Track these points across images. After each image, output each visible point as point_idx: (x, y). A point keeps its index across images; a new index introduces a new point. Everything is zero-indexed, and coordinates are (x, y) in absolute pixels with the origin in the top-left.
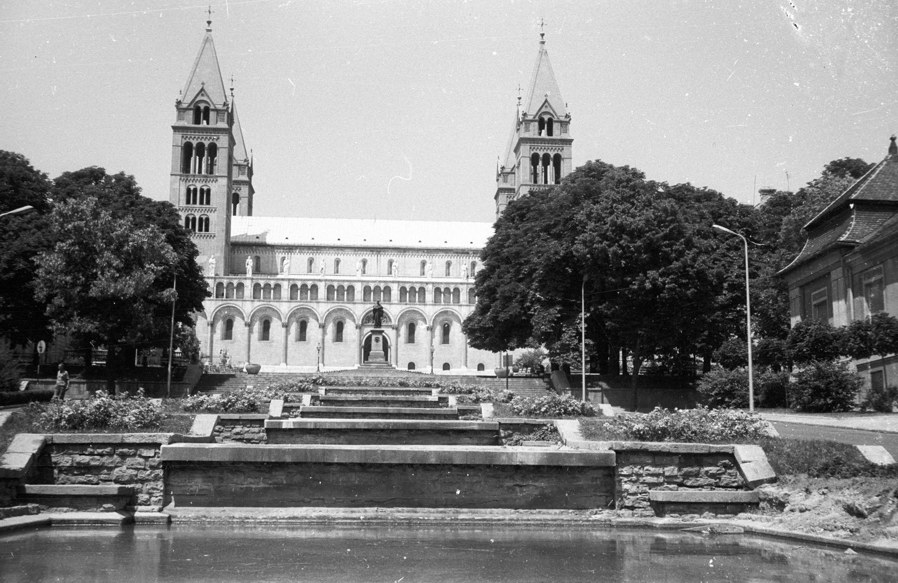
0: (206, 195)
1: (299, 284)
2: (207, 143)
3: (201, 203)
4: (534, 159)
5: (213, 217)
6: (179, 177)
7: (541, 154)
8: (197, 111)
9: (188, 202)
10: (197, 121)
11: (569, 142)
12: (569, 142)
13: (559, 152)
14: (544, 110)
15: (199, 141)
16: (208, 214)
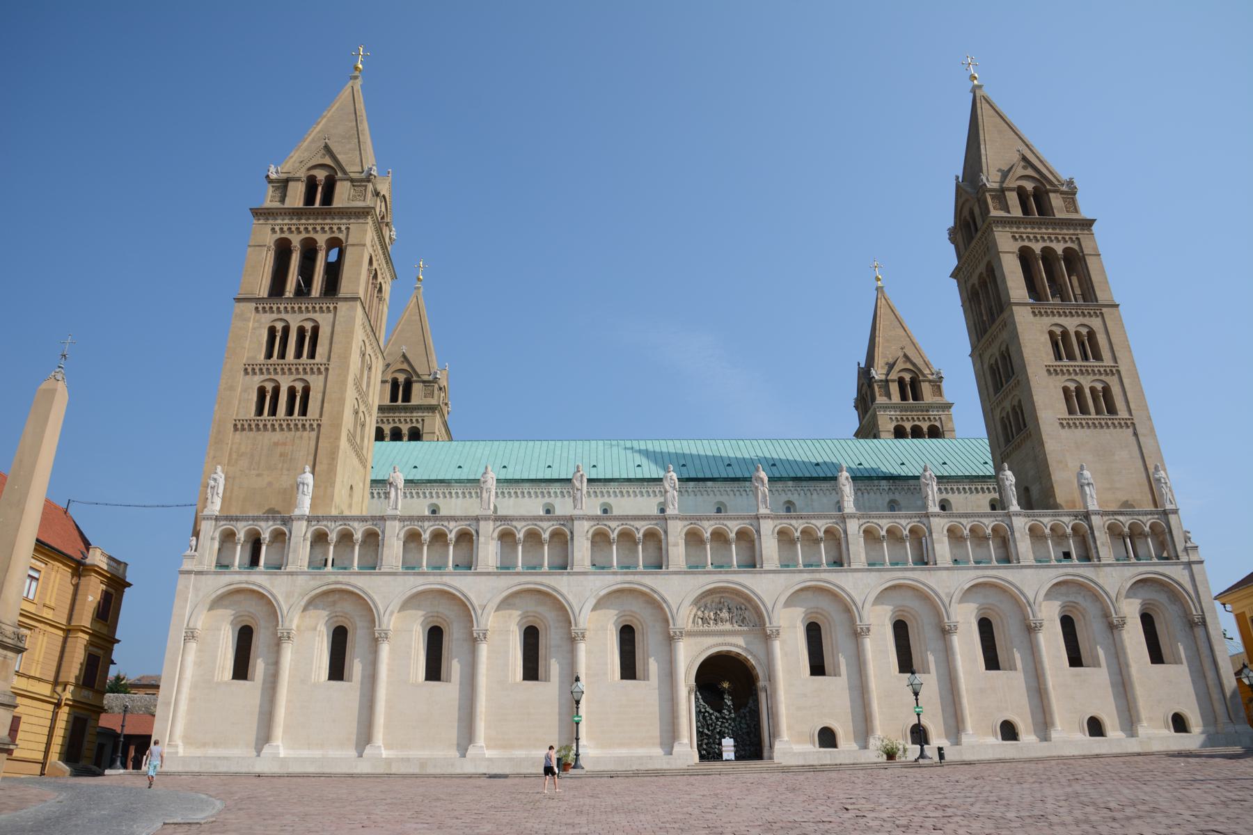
0: (309, 339)
1: (521, 532)
2: (321, 239)
3: (299, 355)
4: (1025, 257)
5: (316, 382)
6: (254, 305)
7: (1037, 247)
8: (311, 185)
9: (269, 355)
10: (310, 199)
11: (1088, 224)
12: (1088, 224)
13: (1069, 244)
14: (1020, 171)
15: (304, 235)
16: (311, 379)
